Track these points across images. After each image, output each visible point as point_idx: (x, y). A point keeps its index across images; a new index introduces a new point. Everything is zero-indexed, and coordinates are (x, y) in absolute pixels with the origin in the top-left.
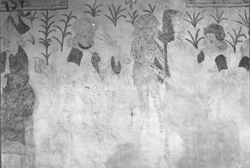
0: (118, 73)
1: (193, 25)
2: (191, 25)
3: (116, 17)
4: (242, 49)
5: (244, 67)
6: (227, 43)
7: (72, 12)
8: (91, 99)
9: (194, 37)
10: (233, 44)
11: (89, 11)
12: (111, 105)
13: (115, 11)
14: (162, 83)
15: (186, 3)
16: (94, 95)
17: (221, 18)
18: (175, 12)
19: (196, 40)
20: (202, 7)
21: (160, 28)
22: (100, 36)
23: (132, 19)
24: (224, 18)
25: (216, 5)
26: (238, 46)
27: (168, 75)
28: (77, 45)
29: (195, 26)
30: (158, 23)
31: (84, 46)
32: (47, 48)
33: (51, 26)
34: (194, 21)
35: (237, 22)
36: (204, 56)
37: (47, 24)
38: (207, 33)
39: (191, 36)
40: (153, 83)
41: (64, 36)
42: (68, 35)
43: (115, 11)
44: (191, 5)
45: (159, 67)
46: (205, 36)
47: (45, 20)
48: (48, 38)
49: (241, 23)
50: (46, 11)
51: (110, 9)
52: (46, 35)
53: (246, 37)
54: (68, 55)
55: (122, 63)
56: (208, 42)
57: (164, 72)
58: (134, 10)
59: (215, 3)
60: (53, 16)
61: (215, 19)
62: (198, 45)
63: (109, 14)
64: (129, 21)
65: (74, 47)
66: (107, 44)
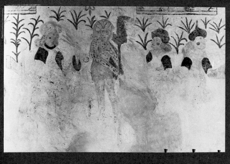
0: (78, 70)
1: (142, 29)
2: (141, 29)
3: (77, 22)
4: (183, 51)
5: (186, 66)
6: (171, 45)
7: (39, 16)
8: (54, 93)
10: (176, 46)
11: (54, 16)
12: (72, 98)
13: (76, 16)
14: (116, 79)
15: (137, 10)
16: (57, 89)
17: (167, 24)
18: (128, 18)
19: (145, 42)
20: (151, 14)
21: (115, 31)
22: (63, 38)
23: (91, 24)
24: (169, 24)
25: (162, 13)
26: (180, 48)
27: (121, 72)
28: (44, 45)
29: (144, 30)
30: (112, 27)
31: (49, 46)
32: (17, 47)
33: (21, 28)
34: (144, 26)
35: (179, 27)
36: (152, 56)
37: (17, 27)
38: (155, 36)
39: (141, 39)
40: (108, 80)
41: (32, 37)
42: (36, 36)
43: (76, 16)
44: (141, 13)
45: (114, 65)
46: (153, 39)
47: (16, 23)
48: (18, 39)
49: (183, 29)
50: (17, 15)
51: (72, 14)
52: (17, 36)
53: (187, 41)
54: (35, 53)
55: (81, 61)
56: (155, 44)
57: (118, 70)
58: (92, 16)
59: (161, 11)
60: (23, 20)
61: (161, 24)
62: (147, 47)
63: (71, 18)
64: (88, 25)
65: (41, 47)
66: (69, 45)
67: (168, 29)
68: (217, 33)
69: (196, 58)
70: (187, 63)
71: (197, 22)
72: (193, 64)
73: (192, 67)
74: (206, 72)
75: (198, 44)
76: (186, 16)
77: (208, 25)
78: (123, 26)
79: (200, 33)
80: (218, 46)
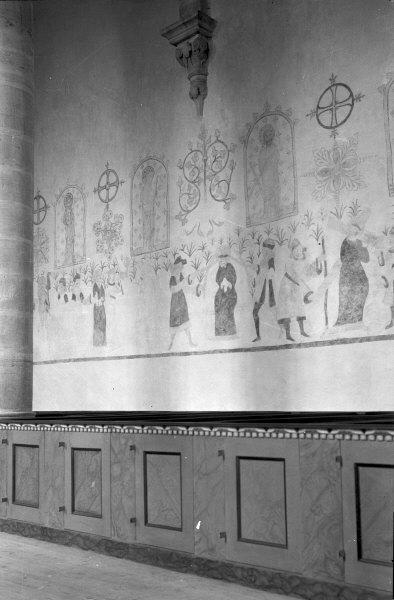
67: (66, 277)
70: (74, 297)
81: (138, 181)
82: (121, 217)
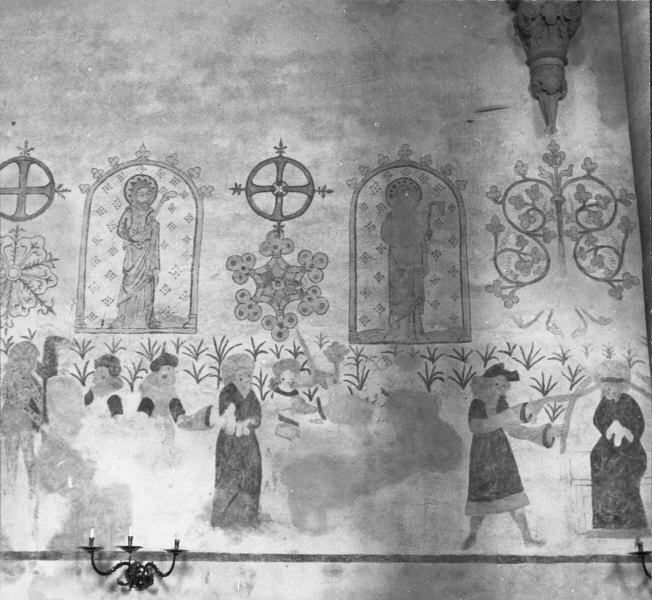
4: (141, 387)
6: (124, 380)
9: (82, 371)
18: (59, 339)
21: (40, 359)
27: (46, 421)
29: (83, 356)
30: (37, 353)
36: (92, 396)
40: (25, 433)
45: (36, 410)
67: (121, 355)
68: (194, 361)
69: (158, 396)
70: (147, 406)
71: (165, 343)
72: (156, 408)
73: (154, 413)
74: (176, 421)
75: (165, 377)
76: (149, 335)
77: (182, 349)
78: (53, 350)
79: (168, 360)
80: (195, 381)
81: (372, 197)
82: (324, 259)
